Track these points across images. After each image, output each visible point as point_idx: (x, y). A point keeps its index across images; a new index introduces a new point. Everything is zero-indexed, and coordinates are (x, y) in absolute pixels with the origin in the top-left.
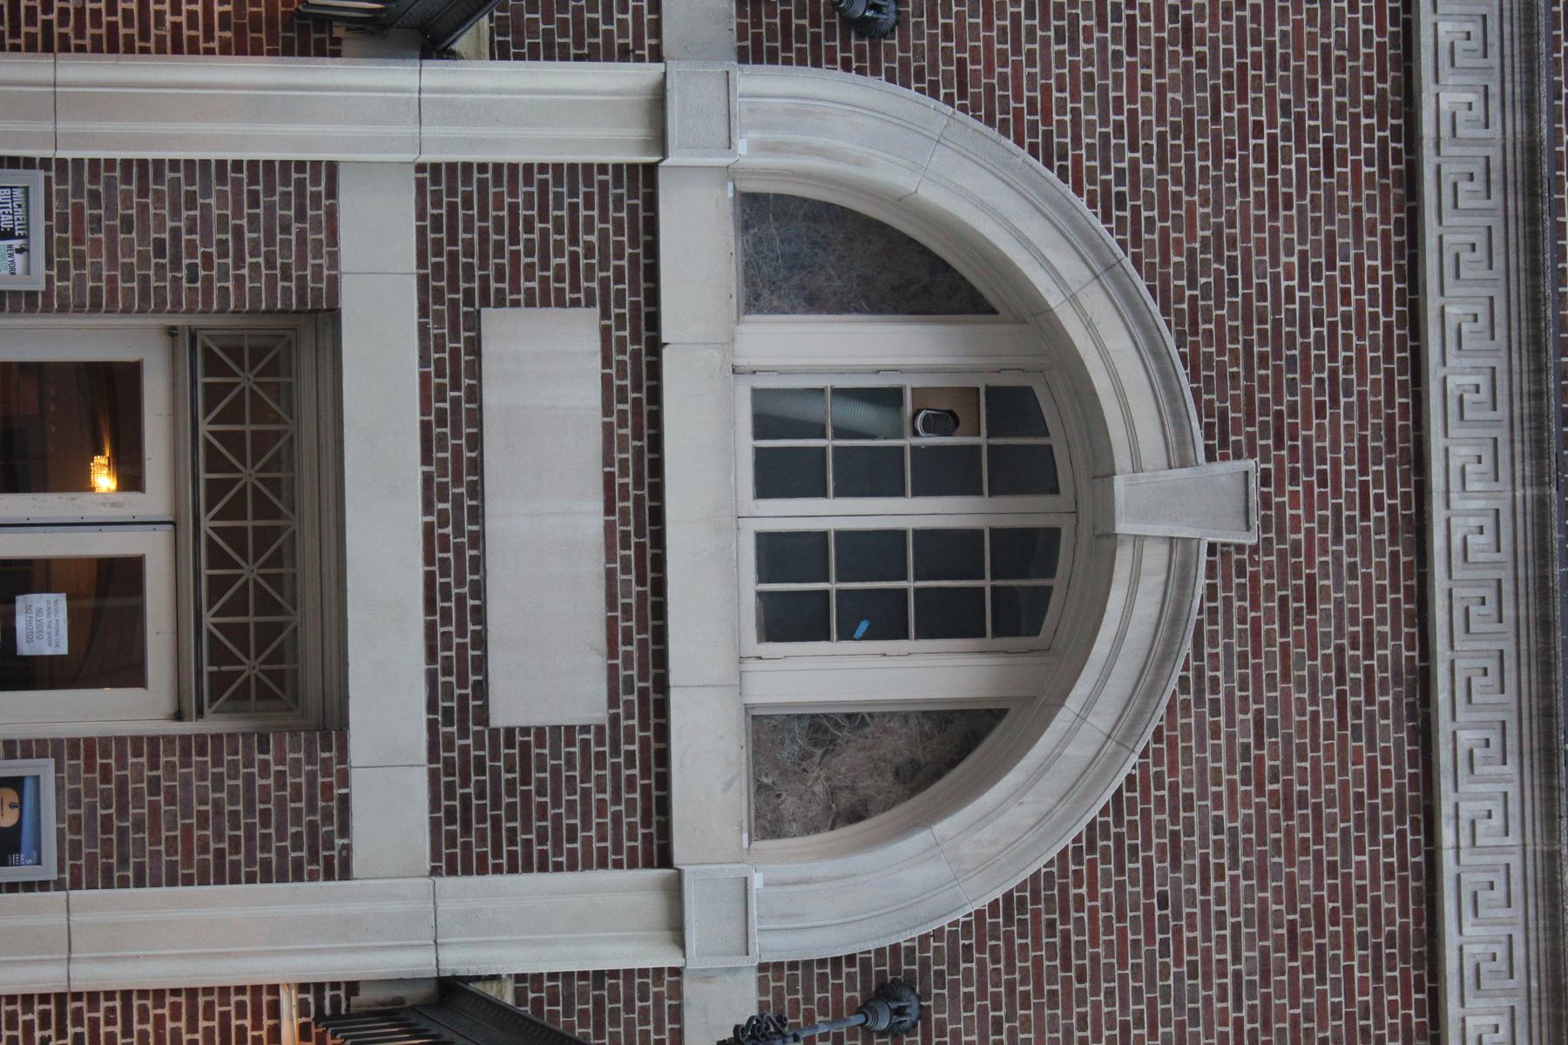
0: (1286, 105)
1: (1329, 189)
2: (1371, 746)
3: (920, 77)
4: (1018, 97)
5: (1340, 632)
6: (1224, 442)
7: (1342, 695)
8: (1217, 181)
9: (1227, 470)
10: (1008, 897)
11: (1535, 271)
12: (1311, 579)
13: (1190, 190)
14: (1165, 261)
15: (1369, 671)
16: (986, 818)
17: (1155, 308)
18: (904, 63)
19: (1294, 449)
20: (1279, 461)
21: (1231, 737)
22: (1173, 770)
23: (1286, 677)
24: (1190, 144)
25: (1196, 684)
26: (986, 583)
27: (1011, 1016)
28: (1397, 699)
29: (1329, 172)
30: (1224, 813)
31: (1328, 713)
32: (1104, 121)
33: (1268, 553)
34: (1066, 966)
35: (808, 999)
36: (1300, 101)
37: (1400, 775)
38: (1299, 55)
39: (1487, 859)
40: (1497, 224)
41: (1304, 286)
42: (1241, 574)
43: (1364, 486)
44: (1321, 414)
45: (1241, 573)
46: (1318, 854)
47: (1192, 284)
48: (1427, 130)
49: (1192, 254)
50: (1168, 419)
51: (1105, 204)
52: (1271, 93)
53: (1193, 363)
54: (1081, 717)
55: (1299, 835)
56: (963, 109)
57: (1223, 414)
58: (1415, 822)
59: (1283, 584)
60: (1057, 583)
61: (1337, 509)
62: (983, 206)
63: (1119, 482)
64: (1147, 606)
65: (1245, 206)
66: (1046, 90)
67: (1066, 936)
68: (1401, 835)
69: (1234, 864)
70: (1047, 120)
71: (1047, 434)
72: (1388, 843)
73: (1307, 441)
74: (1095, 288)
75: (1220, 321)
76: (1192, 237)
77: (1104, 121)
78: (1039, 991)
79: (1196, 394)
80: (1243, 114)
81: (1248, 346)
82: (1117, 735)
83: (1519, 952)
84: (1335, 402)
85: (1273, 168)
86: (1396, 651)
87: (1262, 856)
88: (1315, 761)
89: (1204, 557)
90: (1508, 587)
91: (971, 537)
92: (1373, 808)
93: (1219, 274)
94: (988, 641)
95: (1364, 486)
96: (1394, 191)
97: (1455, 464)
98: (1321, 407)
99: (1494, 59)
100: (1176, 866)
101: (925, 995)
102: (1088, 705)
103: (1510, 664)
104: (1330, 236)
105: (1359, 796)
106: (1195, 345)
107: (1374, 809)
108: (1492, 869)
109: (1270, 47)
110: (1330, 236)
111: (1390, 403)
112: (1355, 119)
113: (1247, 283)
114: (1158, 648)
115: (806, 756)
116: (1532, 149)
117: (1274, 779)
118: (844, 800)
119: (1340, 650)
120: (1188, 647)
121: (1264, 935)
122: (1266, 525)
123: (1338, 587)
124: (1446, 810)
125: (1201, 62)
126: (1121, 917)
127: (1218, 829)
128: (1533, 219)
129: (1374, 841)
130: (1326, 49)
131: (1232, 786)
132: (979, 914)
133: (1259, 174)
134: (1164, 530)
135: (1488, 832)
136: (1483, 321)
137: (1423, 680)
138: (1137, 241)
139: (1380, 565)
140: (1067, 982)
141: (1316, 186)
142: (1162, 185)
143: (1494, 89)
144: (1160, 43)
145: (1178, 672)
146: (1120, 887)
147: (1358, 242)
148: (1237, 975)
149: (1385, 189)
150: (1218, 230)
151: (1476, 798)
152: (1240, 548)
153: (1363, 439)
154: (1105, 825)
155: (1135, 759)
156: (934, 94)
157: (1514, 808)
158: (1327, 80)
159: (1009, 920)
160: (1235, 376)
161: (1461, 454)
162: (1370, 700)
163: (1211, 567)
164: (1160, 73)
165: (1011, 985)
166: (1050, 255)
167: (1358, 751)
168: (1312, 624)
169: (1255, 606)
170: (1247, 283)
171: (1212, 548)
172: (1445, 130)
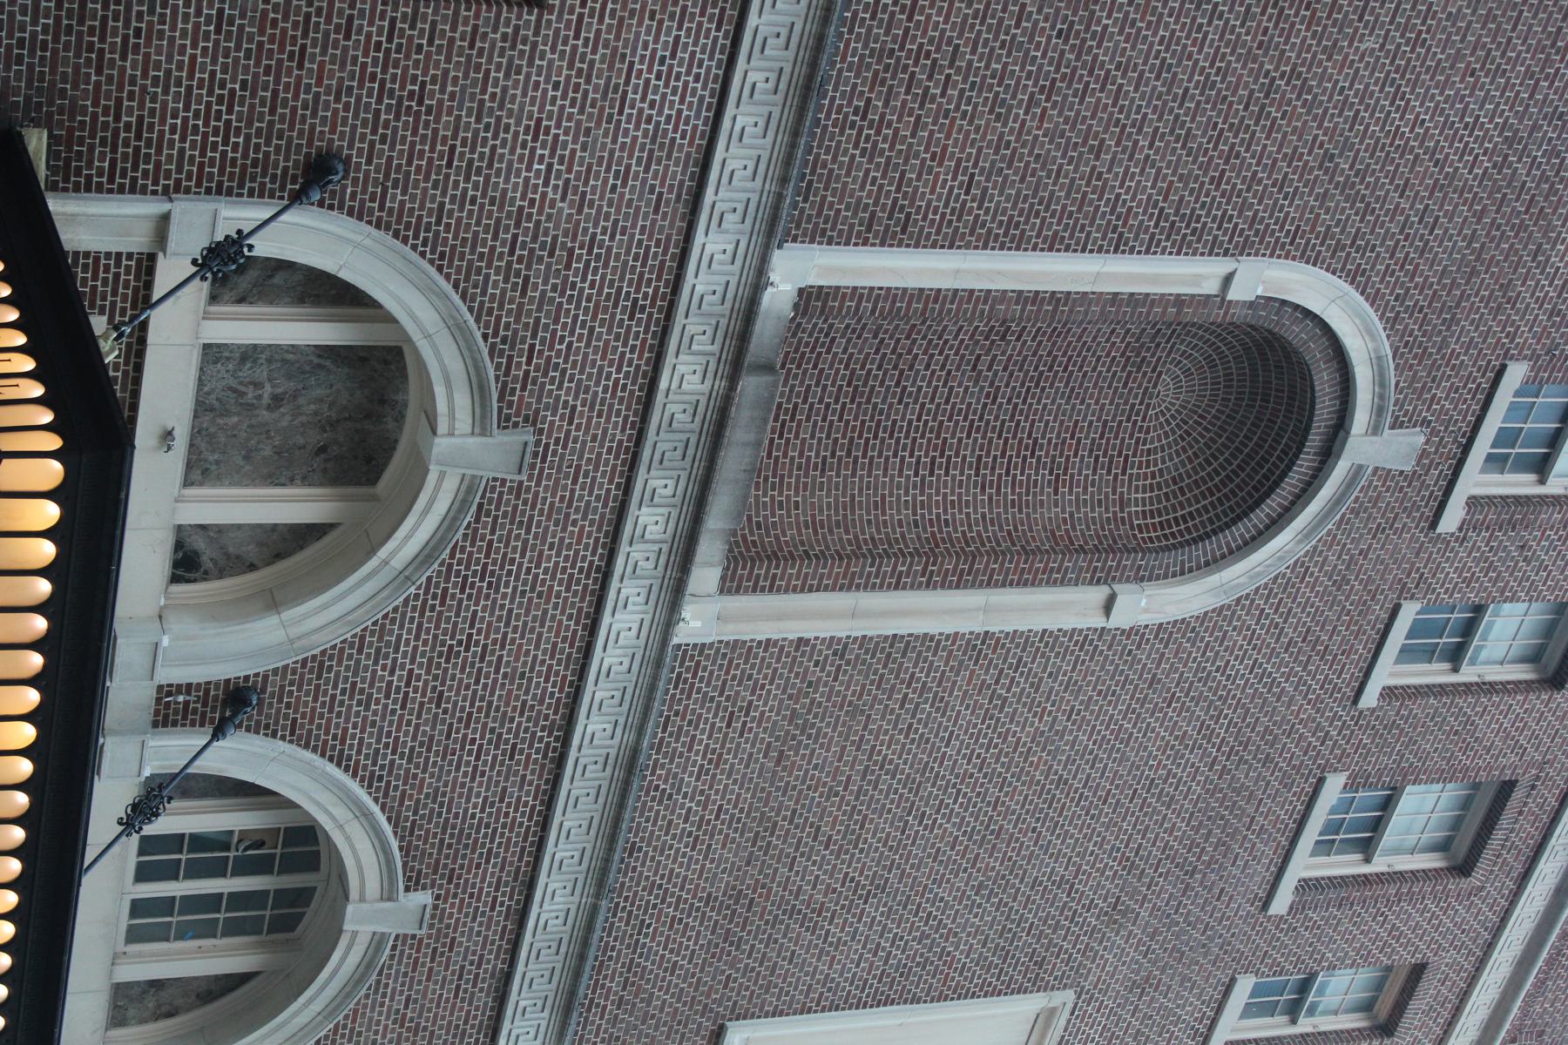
0: (492, 730)
3: (267, 727)
6: (417, 883)
8: (442, 767)
11: (621, 806)
14: (401, 804)
18: (258, 723)
38: (507, 704)
40: (605, 784)
48: (576, 742)
51: (369, 783)
52: (485, 725)
53: (405, 851)
56: (291, 742)
60: (310, 912)
63: (350, 908)
64: (354, 958)
66: (345, 730)
74: (356, 824)
77: (378, 741)
79: (405, 865)
84: (488, 862)
91: (263, 894)
94: (263, 937)
97: (549, 890)
104: (504, 789)
106: (410, 842)
109: (490, 703)
110: (504, 789)
114: (357, 976)
115: (144, 992)
116: (635, 751)
118: (164, 1009)
120: (374, 977)
125: (445, 711)
134: (373, 928)
137: (507, 977)
138: (386, 795)
143: (622, 721)
144: (422, 704)
149: (543, 766)
156: (274, 735)
160: (431, 854)
163: (394, 948)
164: (419, 717)
166: (331, 809)
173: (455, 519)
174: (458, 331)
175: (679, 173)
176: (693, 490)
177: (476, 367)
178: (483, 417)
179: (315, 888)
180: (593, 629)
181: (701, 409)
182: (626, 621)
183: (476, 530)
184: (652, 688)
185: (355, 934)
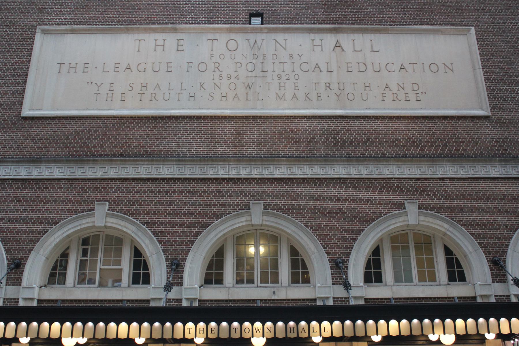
10: (3, 245)
27: (22, 245)
34: (16, 236)
35: (13, 278)
39: (12, 171)
55: (3, 200)
67: (11, 237)
69: (6, 210)
78: (19, 241)
83: (27, 167)
87: (6, 205)
100: (4, 219)
101: (16, 259)
121: (17, 205)
126: (10, 228)
132: (5, 250)
135: (8, 171)
140: (18, 236)
146: (6, 228)
148: (23, 210)
159: (7, 245)
165: (17, 245)
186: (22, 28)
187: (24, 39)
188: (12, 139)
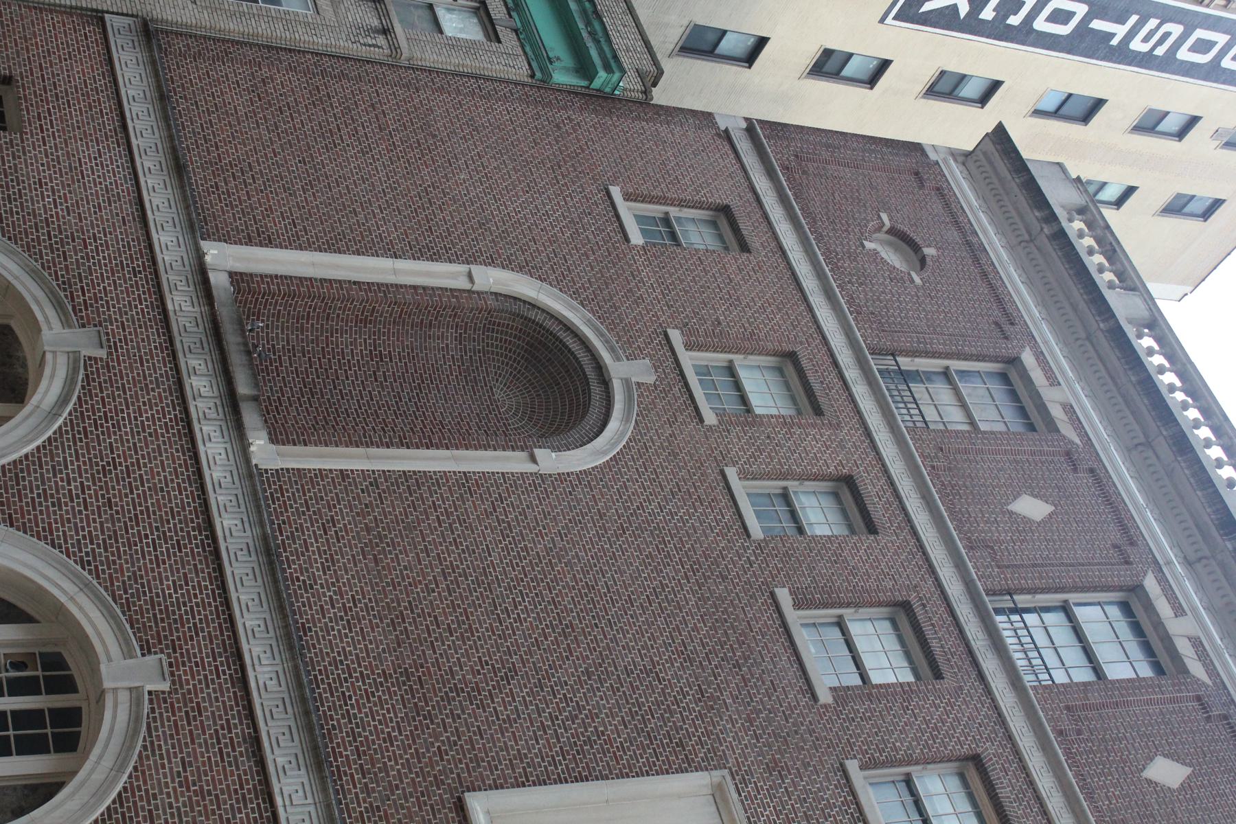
0: (157, 528)
1: (181, 557)
2: (238, 769)
4: (37, 526)
5: (215, 724)
7: (220, 749)
9: (151, 659)
11: (275, 581)
12: (198, 703)
13: (120, 558)
14: (112, 584)
15: (231, 738)
16: (57, 807)
17: (110, 599)
19: (182, 654)
20: (176, 658)
21: (171, 769)
22: (145, 783)
23: (193, 743)
24: (117, 542)
25: (150, 747)
26: (49, 731)
28: (246, 749)
29: (180, 551)
30: (172, 800)
31: (215, 756)
32: (78, 534)
33: (177, 693)
36: (163, 526)
37: (253, 780)
38: (160, 510)
39: (299, 809)
41: (176, 592)
42: (165, 702)
43: (216, 667)
44: (192, 639)
45: (165, 702)
46: (220, 815)
47: (126, 592)
49: (124, 582)
50: (121, 641)
52: (150, 524)
54: (97, 762)
57: (147, 641)
58: (264, 799)
59: (186, 706)
61: (206, 676)
62: (26, 565)
63: (103, 667)
65: (145, 564)
68: (258, 804)
70: (51, 534)
71: (69, 669)
72: (253, 809)
73: (187, 650)
74: (81, 594)
75: (140, 606)
76: (123, 575)
79: (134, 633)
80: (139, 531)
81: (155, 615)
82: (116, 768)
84: (197, 635)
85: (155, 550)
86: (243, 730)
88: (213, 777)
89: (146, 696)
90: (287, 701)
91: (40, 712)
92: (243, 795)
93: (137, 589)
95: (216, 667)
96: (210, 558)
98: (191, 637)
99: (243, 508)
102: (101, 757)
103: (294, 730)
104: (185, 574)
105: (236, 790)
107: (243, 795)
108: (302, 813)
109: (147, 508)
111: (222, 634)
112: (188, 533)
113: (151, 592)
114: (130, 732)
116: (265, 538)
117: (194, 785)
119: (216, 731)
122: (174, 683)
123: (211, 706)
124: (276, 790)
125: (117, 512)
127: (171, 807)
128: (271, 563)
129: (246, 808)
130: (171, 508)
131: (174, 788)
133: (149, 553)
136: (257, 600)
137: (257, 741)
139: (229, 697)
141: (175, 556)
142: (107, 557)
143: (245, 519)
144: (98, 507)
145: (140, 743)
147: (197, 576)
149: (206, 558)
150: (134, 573)
151: (289, 785)
152: (163, 692)
153: (213, 649)
154: (115, 809)
155: (125, 778)
157: (307, 788)
158: (174, 518)
161: (256, 650)
162: (234, 750)
164: (100, 517)
167: (232, 771)
168: (202, 722)
169: (174, 715)
170: (151, 592)
171: (150, 693)
172: (227, 533)
173: (72, 379)
174: (34, 274)
175: (129, 209)
176: (218, 367)
177: (52, 292)
178: (67, 321)
179: (76, 691)
180: (196, 457)
181: (200, 321)
182: (214, 448)
183: (90, 391)
184: (255, 493)
185: (115, 690)
186: (708, 734)
187: (680, 744)
188: (392, 788)
